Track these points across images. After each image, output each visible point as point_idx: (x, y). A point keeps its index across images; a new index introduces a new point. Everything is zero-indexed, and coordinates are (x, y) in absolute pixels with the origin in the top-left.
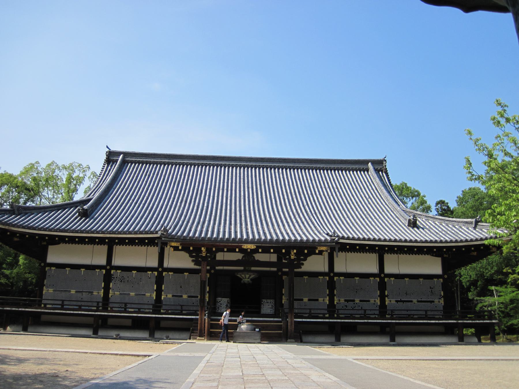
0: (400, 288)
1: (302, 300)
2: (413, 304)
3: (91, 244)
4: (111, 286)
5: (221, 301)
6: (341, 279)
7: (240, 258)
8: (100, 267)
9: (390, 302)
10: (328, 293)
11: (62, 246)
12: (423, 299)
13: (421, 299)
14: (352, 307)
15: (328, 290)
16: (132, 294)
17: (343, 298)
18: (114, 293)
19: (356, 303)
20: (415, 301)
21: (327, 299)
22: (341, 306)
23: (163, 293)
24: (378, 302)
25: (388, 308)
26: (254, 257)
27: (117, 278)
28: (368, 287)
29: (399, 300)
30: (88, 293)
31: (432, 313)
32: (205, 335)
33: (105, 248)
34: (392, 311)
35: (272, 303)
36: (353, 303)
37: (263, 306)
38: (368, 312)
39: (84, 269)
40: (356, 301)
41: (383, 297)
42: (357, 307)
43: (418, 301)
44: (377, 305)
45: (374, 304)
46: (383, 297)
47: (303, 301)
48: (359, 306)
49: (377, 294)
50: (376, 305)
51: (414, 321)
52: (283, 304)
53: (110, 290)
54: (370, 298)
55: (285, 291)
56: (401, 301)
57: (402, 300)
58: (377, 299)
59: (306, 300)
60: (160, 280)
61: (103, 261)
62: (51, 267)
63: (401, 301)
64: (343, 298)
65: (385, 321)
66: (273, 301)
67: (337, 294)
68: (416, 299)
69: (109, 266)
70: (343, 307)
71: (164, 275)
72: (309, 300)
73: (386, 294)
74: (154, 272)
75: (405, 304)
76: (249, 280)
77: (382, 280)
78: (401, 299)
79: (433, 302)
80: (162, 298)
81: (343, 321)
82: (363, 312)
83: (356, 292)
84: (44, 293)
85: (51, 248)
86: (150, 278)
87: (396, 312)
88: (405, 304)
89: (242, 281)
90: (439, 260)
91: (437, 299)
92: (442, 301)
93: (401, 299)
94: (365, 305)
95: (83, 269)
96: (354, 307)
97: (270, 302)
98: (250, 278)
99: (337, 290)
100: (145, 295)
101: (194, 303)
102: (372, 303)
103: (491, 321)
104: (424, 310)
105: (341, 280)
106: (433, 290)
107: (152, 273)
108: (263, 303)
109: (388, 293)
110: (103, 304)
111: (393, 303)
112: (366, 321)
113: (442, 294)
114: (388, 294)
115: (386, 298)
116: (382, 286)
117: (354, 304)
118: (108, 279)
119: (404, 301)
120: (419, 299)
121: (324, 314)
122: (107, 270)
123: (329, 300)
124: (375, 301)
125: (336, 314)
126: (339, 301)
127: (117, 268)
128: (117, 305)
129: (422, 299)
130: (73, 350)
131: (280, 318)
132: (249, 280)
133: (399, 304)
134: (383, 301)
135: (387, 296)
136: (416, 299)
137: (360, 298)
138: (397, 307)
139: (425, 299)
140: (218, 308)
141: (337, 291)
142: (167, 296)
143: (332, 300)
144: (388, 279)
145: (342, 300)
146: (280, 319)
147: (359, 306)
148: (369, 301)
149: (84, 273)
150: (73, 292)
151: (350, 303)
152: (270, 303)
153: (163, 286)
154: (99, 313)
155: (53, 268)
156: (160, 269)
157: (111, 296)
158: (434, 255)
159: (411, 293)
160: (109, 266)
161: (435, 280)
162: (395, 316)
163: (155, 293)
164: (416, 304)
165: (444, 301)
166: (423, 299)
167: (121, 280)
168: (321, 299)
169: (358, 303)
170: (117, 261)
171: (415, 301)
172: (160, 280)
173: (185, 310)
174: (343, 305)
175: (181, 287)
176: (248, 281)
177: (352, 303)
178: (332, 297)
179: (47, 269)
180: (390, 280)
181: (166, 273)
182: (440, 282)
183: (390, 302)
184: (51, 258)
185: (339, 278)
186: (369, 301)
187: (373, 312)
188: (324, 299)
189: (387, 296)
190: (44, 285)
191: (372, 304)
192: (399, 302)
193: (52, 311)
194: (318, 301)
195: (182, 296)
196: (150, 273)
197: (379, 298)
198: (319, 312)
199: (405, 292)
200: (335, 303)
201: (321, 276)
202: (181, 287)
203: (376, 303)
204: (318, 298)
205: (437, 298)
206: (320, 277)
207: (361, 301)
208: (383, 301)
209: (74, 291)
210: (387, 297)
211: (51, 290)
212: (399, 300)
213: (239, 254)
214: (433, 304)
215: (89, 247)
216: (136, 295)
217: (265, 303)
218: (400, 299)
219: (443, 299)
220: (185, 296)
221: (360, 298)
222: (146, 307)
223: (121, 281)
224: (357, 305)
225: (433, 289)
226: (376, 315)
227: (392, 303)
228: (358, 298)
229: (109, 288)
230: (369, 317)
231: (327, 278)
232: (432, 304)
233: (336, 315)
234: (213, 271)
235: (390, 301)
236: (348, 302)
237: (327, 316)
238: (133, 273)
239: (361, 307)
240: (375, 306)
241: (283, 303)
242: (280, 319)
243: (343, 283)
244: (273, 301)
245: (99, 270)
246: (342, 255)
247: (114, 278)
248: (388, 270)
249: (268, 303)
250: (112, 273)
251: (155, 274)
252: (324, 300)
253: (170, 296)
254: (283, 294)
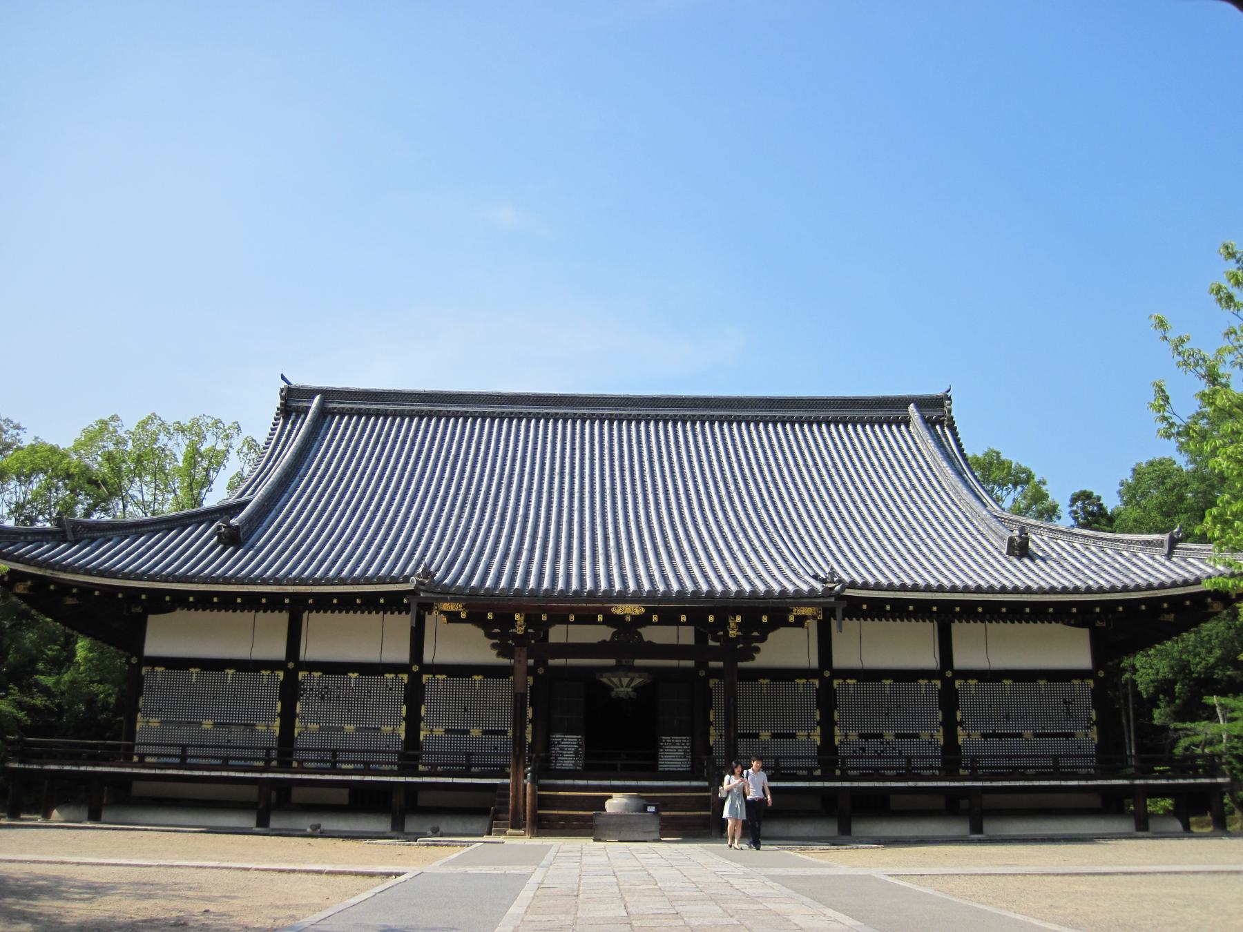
0: (991, 705)
1: (756, 736)
2: (1022, 741)
3: (250, 611)
4: (298, 710)
5: (563, 741)
6: (848, 685)
7: (608, 639)
8: (272, 665)
9: (969, 738)
10: (818, 718)
11: (180, 615)
12: (1048, 729)
13: (1043, 728)
14: (876, 751)
15: (818, 712)
16: (350, 728)
17: (855, 730)
18: (306, 728)
19: (886, 742)
20: (1028, 733)
21: (815, 734)
22: (850, 750)
23: (422, 724)
24: (940, 737)
25: (964, 752)
26: (640, 635)
27: (311, 690)
28: (915, 702)
29: (991, 731)
30: (243, 727)
31: (1070, 763)
32: (525, 824)
33: (281, 619)
34: (973, 759)
35: (685, 745)
36: (880, 742)
37: (664, 751)
38: (915, 763)
39: (234, 669)
40: (885, 737)
41: (950, 726)
42: (890, 750)
44: (938, 744)
45: (930, 743)
46: (950, 726)
47: (758, 738)
48: (894, 749)
49: (936, 719)
50: (935, 744)
51: (1026, 783)
52: (712, 747)
53: (297, 720)
54: (919, 730)
55: (716, 715)
56: (994, 735)
57: (998, 733)
58: (938, 731)
59: (765, 735)
60: (414, 695)
61: (278, 651)
62: (154, 666)
63: (994, 735)
64: (855, 730)
65: (957, 784)
66: (686, 739)
67: (840, 721)
68: (1030, 730)
69: (293, 663)
70: (854, 751)
71: (424, 681)
72: (774, 736)
73: (959, 718)
74: (400, 676)
75: (1005, 741)
76: (630, 690)
77: (948, 685)
78: (994, 731)
79: (1072, 735)
80: (422, 738)
81: (856, 784)
82: (903, 762)
83: (887, 714)
84: (138, 729)
85: (154, 622)
86: (391, 689)
87: (983, 762)
88: (1005, 741)
89: (613, 694)
90: (1083, 635)
91: (1082, 729)
92: (1094, 734)
93: (994, 731)
94: (909, 747)
95: (230, 669)
96: (882, 751)
97: (681, 743)
98: (632, 685)
99: (840, 710)
100: (379, 729)
101: (498, 747)
102: (926, 741)
103: (1213, 781)
104: (1049, 756)
105: (848, 688)
106: (1072, 707)
107: (396, 676)
108: (662, 744)
109: (962, 716)
110: (280, 754)
111: (976, 741)
112: (911, 784)
113: (1094, 717)
114: (962, 718)
115: (959, 728)
116: (949, 700)
117: (882, 743)
118: (290, 692)
119: (1000, 736)
120: (1039, 729)
121: (810, 770)
122: (287, 672)
123: (822, 736)
124: (932, 736)
125: (840, 769)
126: (846, 738)
127: (313, 666)
128: (314, 755)
129: (1045, 729)
130: (215, 864)
131: (704, 780)
132: (630, 690)
133: (990, 741)
134: (950, 735)
135: (961, 723)
136: (1030, 730)
137: (895, 730)
138: (985, 749)
139: (1053, 729)
140: (556, 757)
141: (840, 713)
142: (432, 731)
143: (827, 736)
144: (963, 681)
145: (853, 736)
146: (706, 784)
147: (893, 747)
148: (917, 736)
149: (233, 680)
150: (208, 724)
151: (871, 742)
152: (681, 745)
153: (423, 707)
154: (271, 775)
155: (159, 669)
156: (415, 668)
157: (299, 734)
158: (1073, 622)
159: (1018, 716)
160: (293, 663)
161: (1076, 682)
162: (980, 772)
163: (404, 724)
164: (1031, 741)
165: (1099, 733)
166: (1048, 729)
167: (321, 694)
168: (802, 734)
169: (892, 741)
170: (311, 651)
171: (1028, 733)
172: (414, 695)
173: (476, 766)
174: (856, 747)
175: (466, 710)
176: (627, 692)
177: (877, 742)
178: (827, 725)
179: (144, 670)
180: (967, 685)
181: (431, 676)
182: (1088, 688)
183: (969, 738)
184: (155, 646)
185: (845, 682)
186: (917, 736)
187: (926, 763)
188: (809, 733)
189: (961, 723)
190: (137, 710)
191: (926, 744)
192: (990, 738)
193: (158, 772)
194: (796, 739)
195: (468, 732)
196: (390, 676)
197: (941, 729)
198: (798, 763)
199: (1003, 713)
200: (837, 743)
201: (801, 679)
202: (466, 710)
203: (934, 742)
204: (796, 730)
205: (1082, 726)
206: (798, 681)
207: (898, 736)
208: (950, 735)
209: (210, 722)
210: (961, 726)
211: (155, 722)
212: (991, 731)
213: (604, 627)
214: (1071, 740)
215: (247, 616)
216: (358, 730)
217: (668, 745)
218: (992, 730)
219: (1095, 728)
220: (476, 732)
221: (895, 730)
222: (381, 758)
223: (323, 698)
224: (890, 747)
225: (1072, 704)
226: (935, 768)
227: (972, 741)
228: (892, 730)
229: (294, 715)
230: (919, 774)
231: (817, 682)
232: (1069, 741)
233: (838, 772)
234: (541, 671)
235: (969, 735)
236: (867, 740)
237: (818, 773)
238: (350, 678)
239: (899, 750)
240: (932, 747)
241: (711, 743)
242: (706, 784)
243: (854, 693)
244: (686, 739)
245: (268, 672)
246: (851, 625)
247: (305, 690)
248: (962, 660)
249: (674, 744)
250: (300, 678)
251: (402, 679)
252: (809, 736)
253: (439, 731)
254: (711, 724)
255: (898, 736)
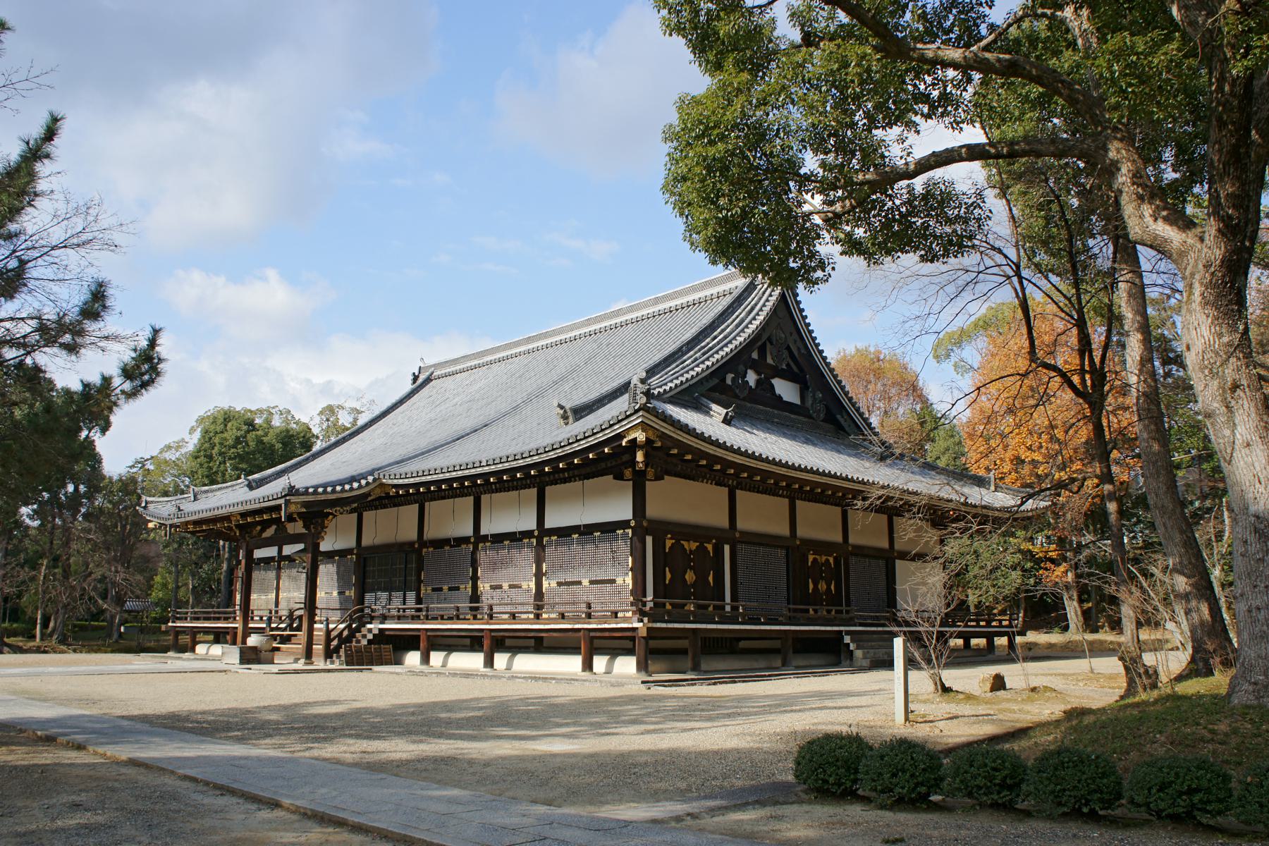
24: (533, 585)
43: (592, 582)
46: (539, 576)
59: (445, 588)
92: (629, 580)
94: (517, 596)
161: (620, 532)
219: (630, 573)
255: (511, 586)
